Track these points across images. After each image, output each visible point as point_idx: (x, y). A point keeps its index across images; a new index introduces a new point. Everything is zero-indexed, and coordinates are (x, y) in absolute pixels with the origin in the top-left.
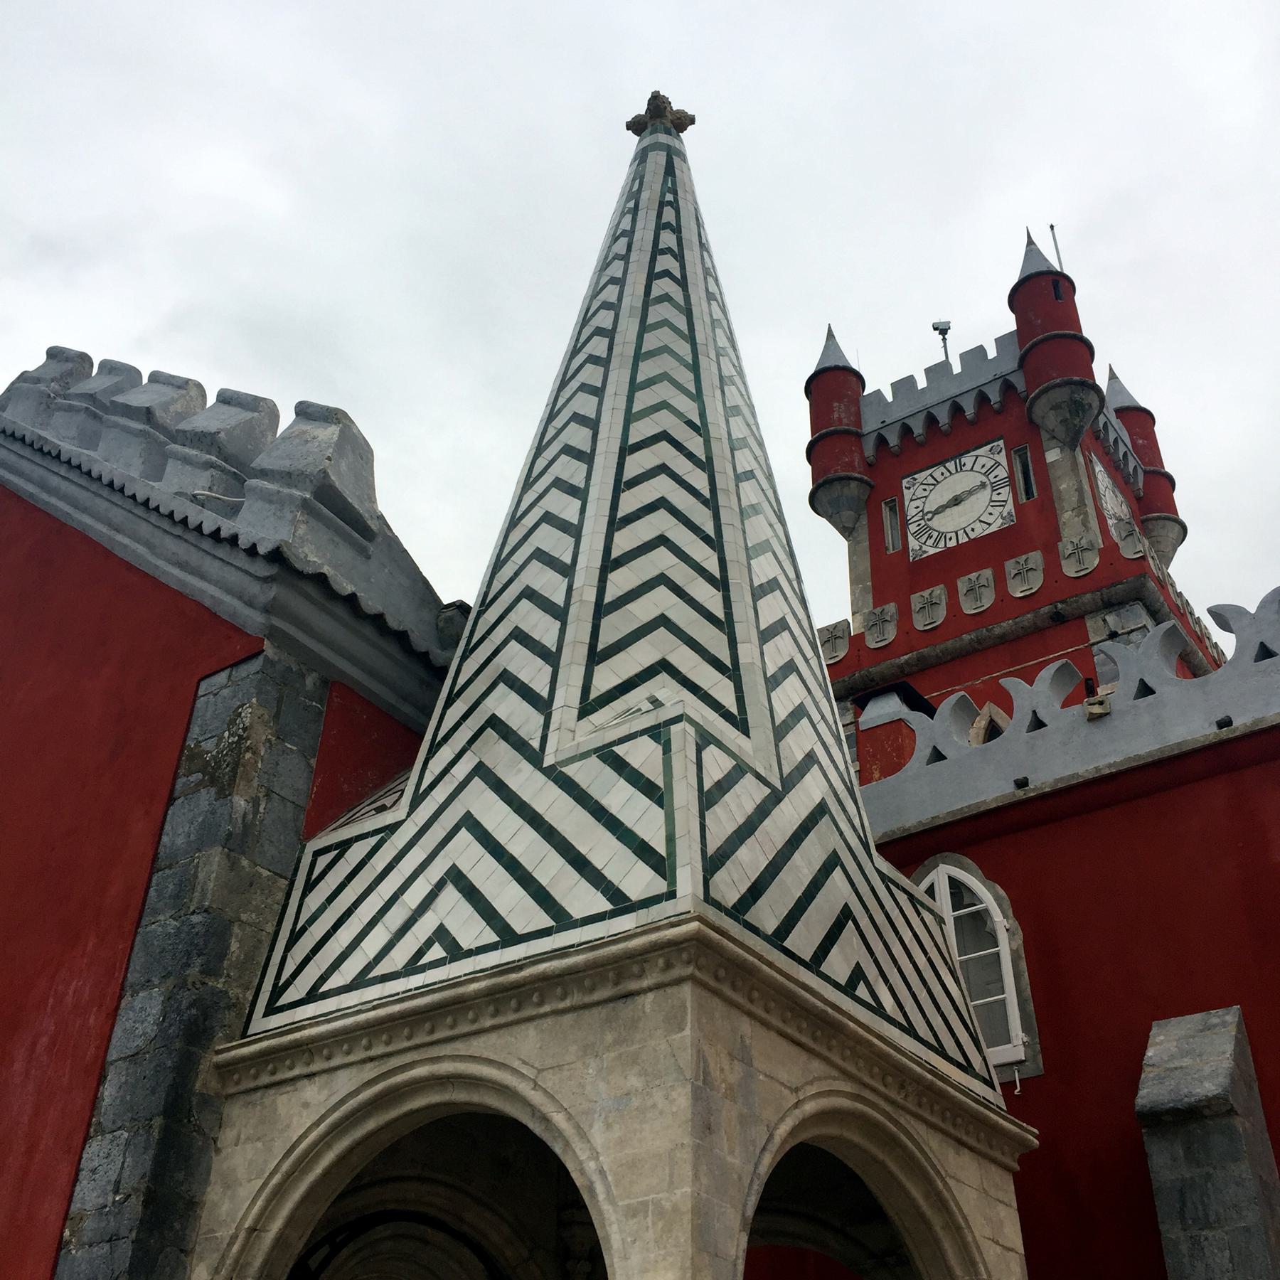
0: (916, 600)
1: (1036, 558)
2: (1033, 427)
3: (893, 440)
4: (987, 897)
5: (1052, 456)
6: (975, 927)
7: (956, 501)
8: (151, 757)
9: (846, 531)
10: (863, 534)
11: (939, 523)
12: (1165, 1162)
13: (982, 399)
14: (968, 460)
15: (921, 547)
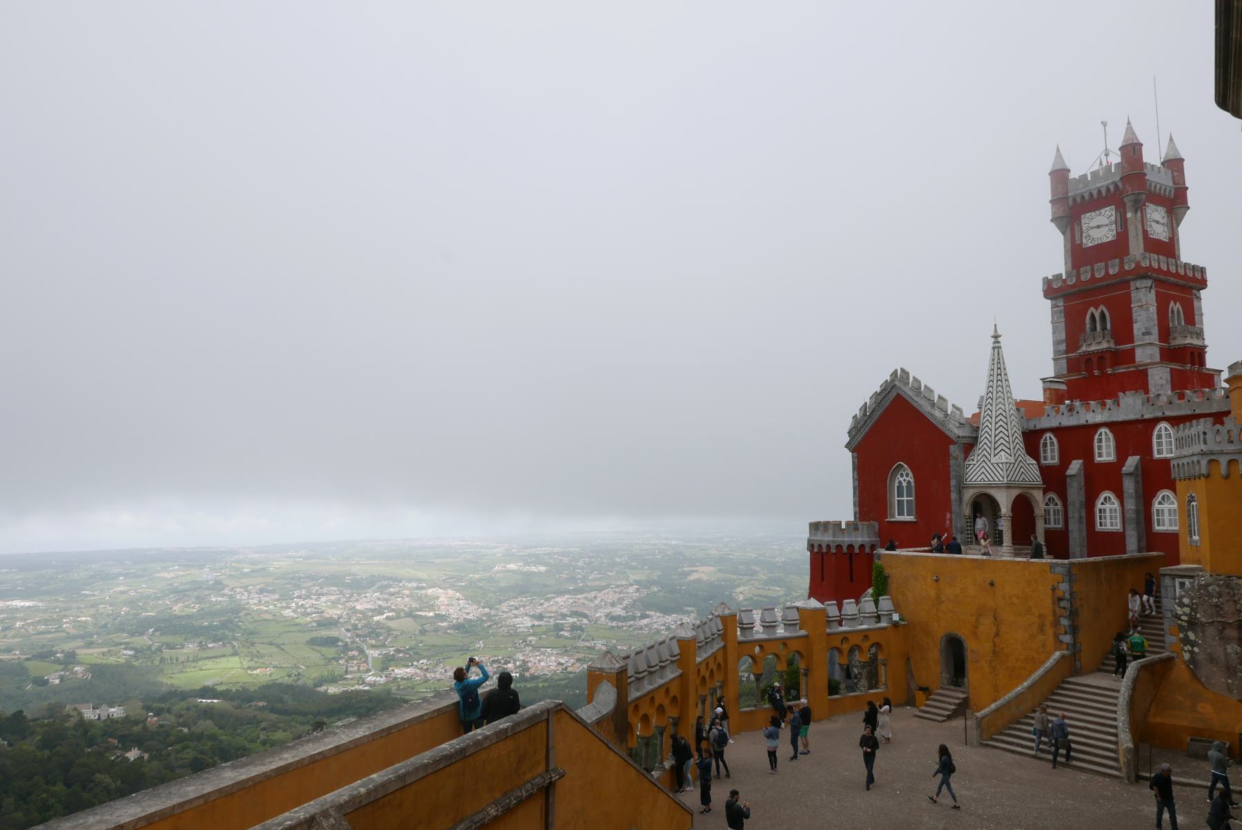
0: (1082, 269)
1: (1117, 261)
2: (1124, 204)
3: (1079, 200)
4: (1054, 440)
5: (1129, 215)
6: (1052, 444)
7: (1098, 227)
8: (946, 455)
9: (1063, 233)
10: (1068, 233)
11: (1091, 232)
12: (1068, 480)
13: (1108, 189)
14: (1103, 211)
15: (1088, 243)
